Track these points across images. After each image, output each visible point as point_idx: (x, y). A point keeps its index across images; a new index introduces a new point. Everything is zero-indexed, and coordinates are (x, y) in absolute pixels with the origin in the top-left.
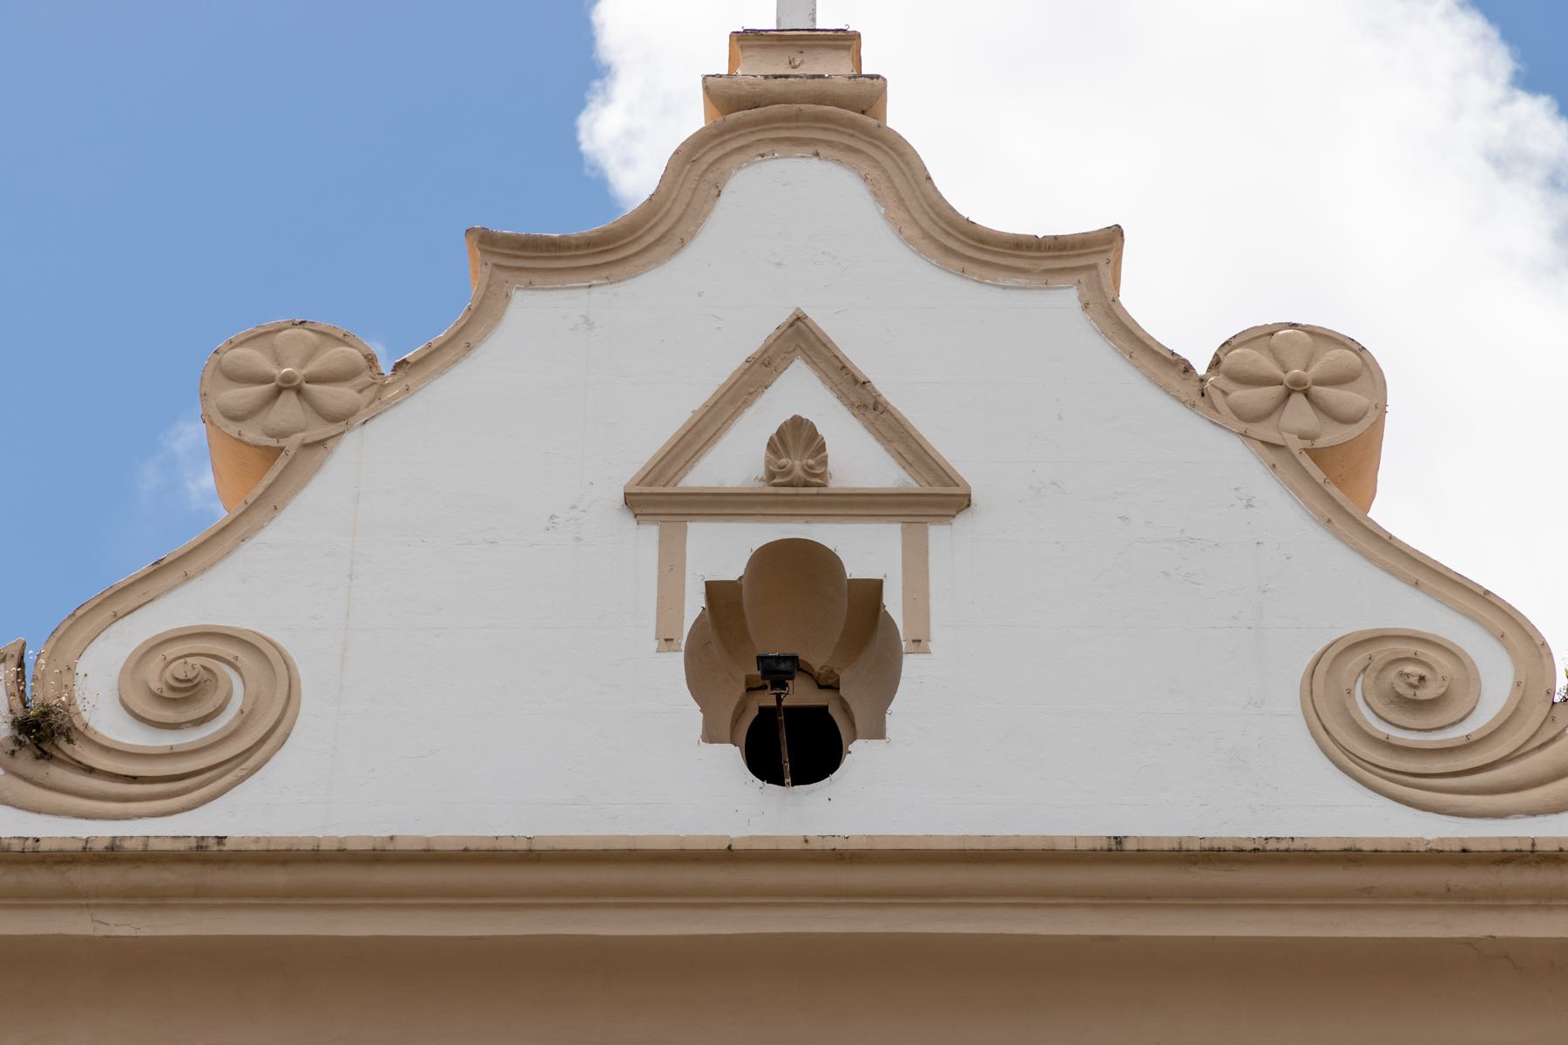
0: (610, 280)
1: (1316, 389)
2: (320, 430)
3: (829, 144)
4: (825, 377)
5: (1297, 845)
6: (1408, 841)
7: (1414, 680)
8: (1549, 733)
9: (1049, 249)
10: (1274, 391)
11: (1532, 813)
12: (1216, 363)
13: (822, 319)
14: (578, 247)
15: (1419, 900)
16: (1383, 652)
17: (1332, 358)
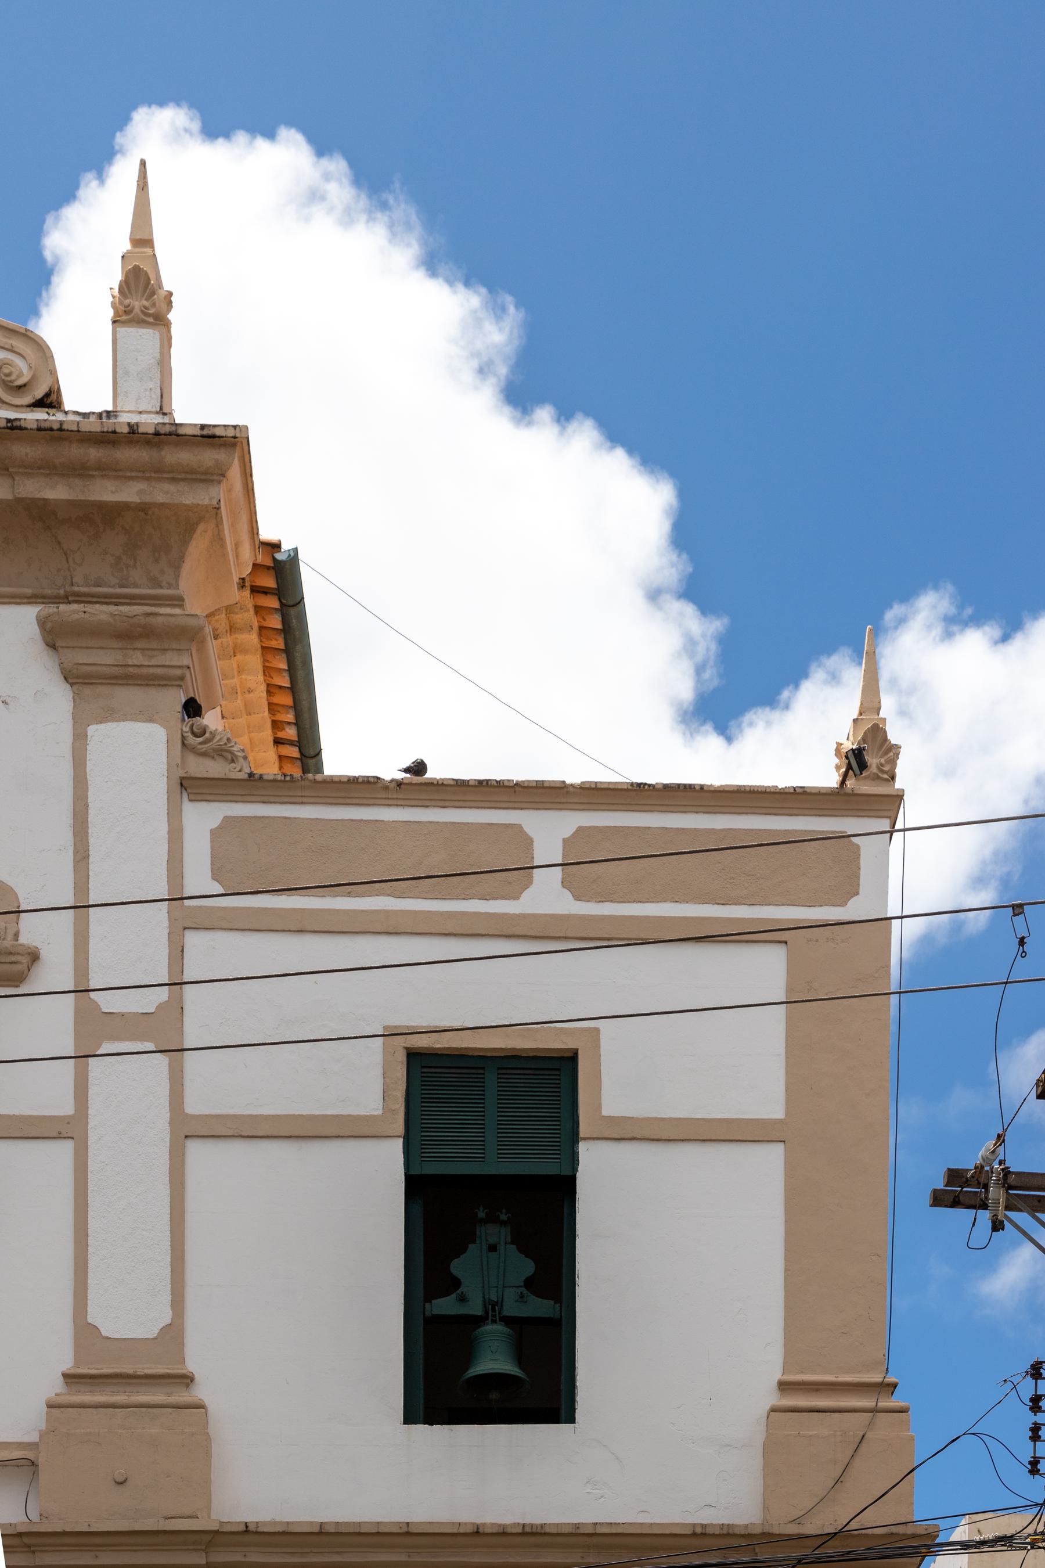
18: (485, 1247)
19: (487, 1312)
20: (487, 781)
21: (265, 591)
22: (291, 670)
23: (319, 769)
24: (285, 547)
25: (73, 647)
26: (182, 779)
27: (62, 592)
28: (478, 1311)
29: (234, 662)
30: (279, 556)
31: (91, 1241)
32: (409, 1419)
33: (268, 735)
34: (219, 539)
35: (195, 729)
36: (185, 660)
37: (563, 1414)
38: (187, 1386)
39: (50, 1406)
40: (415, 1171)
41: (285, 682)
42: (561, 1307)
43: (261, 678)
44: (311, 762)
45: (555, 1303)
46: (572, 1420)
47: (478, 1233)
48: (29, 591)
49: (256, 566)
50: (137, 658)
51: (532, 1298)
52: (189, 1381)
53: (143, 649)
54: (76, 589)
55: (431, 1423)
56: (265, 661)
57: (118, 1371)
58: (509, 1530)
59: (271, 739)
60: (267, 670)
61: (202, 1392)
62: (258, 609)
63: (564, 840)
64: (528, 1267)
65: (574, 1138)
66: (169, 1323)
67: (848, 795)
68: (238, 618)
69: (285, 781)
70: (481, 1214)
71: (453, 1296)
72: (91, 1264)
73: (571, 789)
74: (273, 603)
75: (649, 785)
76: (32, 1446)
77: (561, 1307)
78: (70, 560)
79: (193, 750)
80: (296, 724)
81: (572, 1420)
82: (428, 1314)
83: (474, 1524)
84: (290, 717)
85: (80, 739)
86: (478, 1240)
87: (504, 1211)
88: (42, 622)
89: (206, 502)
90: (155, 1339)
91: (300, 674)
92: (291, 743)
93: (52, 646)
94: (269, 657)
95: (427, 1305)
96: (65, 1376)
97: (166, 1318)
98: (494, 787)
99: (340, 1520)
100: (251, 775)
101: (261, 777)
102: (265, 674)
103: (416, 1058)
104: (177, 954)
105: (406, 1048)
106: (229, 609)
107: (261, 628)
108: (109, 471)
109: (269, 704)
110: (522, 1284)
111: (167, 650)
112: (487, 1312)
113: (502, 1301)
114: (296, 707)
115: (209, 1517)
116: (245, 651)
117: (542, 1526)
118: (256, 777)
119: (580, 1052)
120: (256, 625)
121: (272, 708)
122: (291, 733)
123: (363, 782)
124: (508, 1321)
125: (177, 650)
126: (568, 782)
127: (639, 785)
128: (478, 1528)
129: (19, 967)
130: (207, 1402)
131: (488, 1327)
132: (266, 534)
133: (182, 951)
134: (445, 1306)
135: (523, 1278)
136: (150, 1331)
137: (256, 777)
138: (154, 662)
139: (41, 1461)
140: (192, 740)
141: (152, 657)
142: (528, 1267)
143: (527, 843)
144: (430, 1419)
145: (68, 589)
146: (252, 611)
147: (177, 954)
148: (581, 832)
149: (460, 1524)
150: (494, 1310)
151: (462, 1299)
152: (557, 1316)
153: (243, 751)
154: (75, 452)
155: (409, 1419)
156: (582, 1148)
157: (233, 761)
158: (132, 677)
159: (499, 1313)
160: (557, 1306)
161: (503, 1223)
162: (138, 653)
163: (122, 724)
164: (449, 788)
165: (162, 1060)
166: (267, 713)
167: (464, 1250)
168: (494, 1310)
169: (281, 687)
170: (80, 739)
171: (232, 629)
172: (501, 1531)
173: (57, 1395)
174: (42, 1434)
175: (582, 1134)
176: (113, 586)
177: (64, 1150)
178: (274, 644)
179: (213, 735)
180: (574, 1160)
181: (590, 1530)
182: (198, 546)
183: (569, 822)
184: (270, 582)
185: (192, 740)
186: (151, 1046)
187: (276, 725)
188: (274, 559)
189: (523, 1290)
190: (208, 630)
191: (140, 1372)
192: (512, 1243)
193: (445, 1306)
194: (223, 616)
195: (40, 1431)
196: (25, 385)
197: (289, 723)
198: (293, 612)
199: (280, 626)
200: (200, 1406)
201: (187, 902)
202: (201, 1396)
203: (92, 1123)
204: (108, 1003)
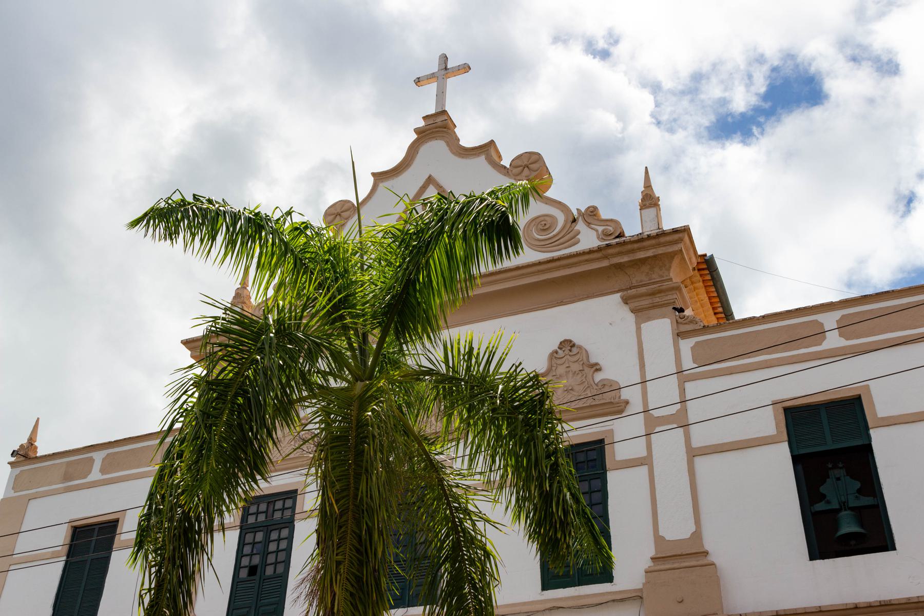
0: (397, 177)
1: (531, 166)
2: (343, 222)
3: (438, 136)
4: (435, 187)
5: (507, 268)
6: (528, 263)
7: (543, 225)
8: (571, 229)
9: (479, 148)
10: (521, 168)
11: (566, 248)
12: (510, 165)
13: (435, 175)
14: (391, 172)
15: (533, 274)
16: (538, 220)
17: (534, 158)
18: (834, 480)
19: (841, 506)
20: (799, 308)
21: (703, 269)
22: (717, 291)
23: (733, 318)
24: (708, 255)
26: (678, 333)
27: (629, 287)
28: (837, 506)
29: (695, 293)
30: (706, 258)
31: (658, 502)
32: (812, 557)
33: (711, 312)
34: (683, 259)
35: (681, 317)
36: (675, 296)
37: (889, 546)
38: (706, 556)
39: (646, 572)
40: (796, 453)
41: (715, 294)
42: (877, 499)
43: (706, 295)
44: (730, 317)
45: (874, 498)
46: (894, 549)
47: (830, 474)
48: (617, 289)
49: (698, 263)
50: (657, 300)
51: (862, 497)
52: (706, 554)
54: (633, 285)
55: (823, 559)
56: (706, 290)
58: (873, 605)
59: (713, 313)
60: (707, 293)
61: (712, 558)
62: (701, 275)
63: (837, 321)
64: (858, 485)
65: (867, 428)
66: (695, 530)
68: (694, 279)
70: (830, 466)
71: (823, 502)
72: (659, 512)
73: (836, 303)
74: (707, 272)
75: (869, 295)
76: (641, 590)
77: (877, 499)
78: (631, 277)
79: (681, 323)
80: (722, 306)
81: (894, 549)
82: (813, 511)
83: (854, 603)
84: (719, 305)
85: (639, 329)
86: (831, 477)
87: (840, 463)
88: (622, 298)
89: (677, 249)
90: (689, 538)
91: (720, 291)
92: (721, 313)
93: (626, 303)
94: (707, 288)
95: (812, 507)
96: (652, 559)
97: (693, 529)
99: (786, 609)
100: (704, 326)
101: (708, 326)
102: (707, 294)
103: (787, 410)
104: (682, 391)
105: (783, 407)
106: (690, 278)
107: (703, 281)
108: (640, 249)
109: (710, 303)
110: (856, 492)
112: (841, 506)
113: (848, 500)
114: (721, 301)
115: (723, 613)
116: (698, 289)
117: (890, 600)
119: (862, 395)
120: (701, 280)
121: (711, 303)
122: (720, 310)
124: (852, 509)
126: (834, 301)
127: (865, 296)
128: (856, 605)
129: (622, 407)
130: (715, 561)
131: (843, 513)
132: (700, 252)
133: (684, 390)
134: (820, 506)
135: (856, 489)
136: (687, 535)
139: (644, 596)
140: (680, 320)
142: (858, 485)
143: (822, 325)
144: (823, 556)
145: (631, 286)
146: (699, 276)
147: (682, 391)
148: (843, 317)
149: (846, 604)
150: (844, 505)
151: (828, 502)
152: (876, 503)
153: (700, 319)
154: (629, 247)
155: (812, 557)
156: (872, 432)
157: (696, 323)
158: (656, 306)
159: (848, 506)
160: (876, 499)
161: (841, 468)
162: (658, 299)
163: (654, 321)
165: (681, 430)
166: (710, 306)
167: (825, 482)
168: (844, 505)
169: (714, 297)
170: (639, 329)
171: (692, 283)
172: (869, 605)
173: (649, 567)
174: (644, 584)
175: (870, 427)
176: (647, 281)
177: (644, 470)
178: (709, 284)
179: (688, 317)
180: (869, 437)
181: (916, 600)
182: (676, 262)
183: (837, 314)
184: (705, 266)
185: (680, 320)
186: (675, 426)
187: (714, 309)
188: (705, 260)
189: (857, 494)
190: (682, 286)
191: (684, 553)
192: (847, 475)
193: (820, 506)
194: (688, 280)
195: (643, 583)
196: (611, 234)
197: (719, 307)
198: (714, 273)
199: (710, 278)
200: (713, 564)
201: (684, 373)
202: (712, 560)
203: (654, 457)
204: (656, 413)
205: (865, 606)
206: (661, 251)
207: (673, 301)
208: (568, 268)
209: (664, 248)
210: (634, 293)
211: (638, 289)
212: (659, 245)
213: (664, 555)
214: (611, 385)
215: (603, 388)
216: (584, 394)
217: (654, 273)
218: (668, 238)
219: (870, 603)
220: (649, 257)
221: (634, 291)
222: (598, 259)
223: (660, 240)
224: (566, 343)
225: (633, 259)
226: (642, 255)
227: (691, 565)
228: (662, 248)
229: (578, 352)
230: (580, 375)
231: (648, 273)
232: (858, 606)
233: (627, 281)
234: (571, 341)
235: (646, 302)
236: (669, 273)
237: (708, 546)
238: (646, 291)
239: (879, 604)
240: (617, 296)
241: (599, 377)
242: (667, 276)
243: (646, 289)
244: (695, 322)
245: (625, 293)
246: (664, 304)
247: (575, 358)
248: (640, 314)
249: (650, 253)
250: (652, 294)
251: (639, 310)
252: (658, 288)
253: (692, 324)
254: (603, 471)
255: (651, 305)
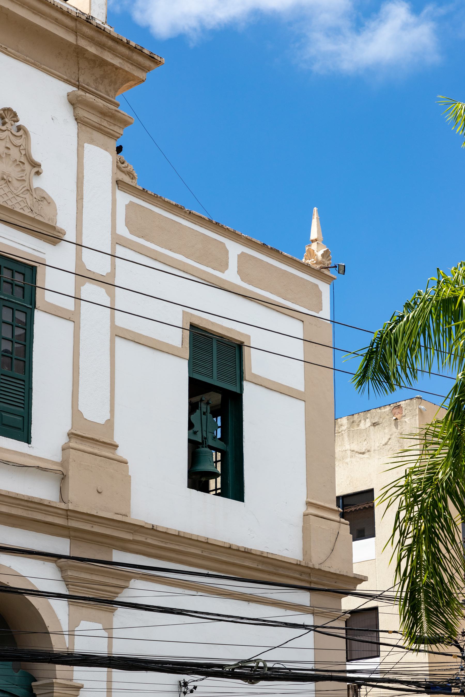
25: (84, 109)
48: (66, 78)
50: (105, 124)
53: (107, 121)
57: (93, 437)
67: (321, 272)
69: (154, 196)
98: (220, 226)
111: (115, 125)
118: (146, 190)
123: (180, 207)
125: (119, 126)
137: (146, 190)
138: (111, 128)
141: (110, 125)
162: (106, 122)
164: (206, 221)
191: (101, 440)
205: (236, 548)
206: (127, 67)
207: (118, 135)
208: (33, 13)
209: (131, 67)
210: (91, 100)
211: (96, 99)
212: (128, 59)
213: (84, 435)
214: (49, 203)
215: (41, 201)
216: (21, 195)
217: (101, 84)
218: (140, 59)
219: (239, 547)
220: (113, 65)
221: (92, 98)
222: (66, 27)
223: (134, 54)
224: (9, 113)
225: (100, 55)
226: (108, 57)
227: (110, 457)
228: (129, 65)
229: (21, 136)
230: (18, 169)
231: (97, 79)
232: (231, 547)
233: (74, 73)
234: (15, 115)
235: (95, 119)
236: (115, 95)
237: (117, 440)
238: (103, 107)
239: (243, 550)
240: (71, 89)
241: (37, 183)
242: (112, 97)
243: (104, 105)
244: (132, 176)
245: (81, 93)
246: (109, 133)
247: (18, 142)
248: (84, 127)
249: (117, 62)
250: (104, 114)
251: (84, 122)
252: (114, 112)
253: (128, 176)
254: (31, 307)
255: (97, 125)
